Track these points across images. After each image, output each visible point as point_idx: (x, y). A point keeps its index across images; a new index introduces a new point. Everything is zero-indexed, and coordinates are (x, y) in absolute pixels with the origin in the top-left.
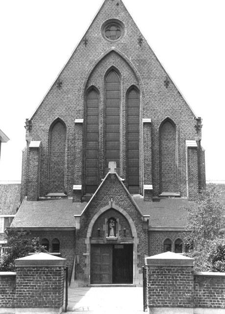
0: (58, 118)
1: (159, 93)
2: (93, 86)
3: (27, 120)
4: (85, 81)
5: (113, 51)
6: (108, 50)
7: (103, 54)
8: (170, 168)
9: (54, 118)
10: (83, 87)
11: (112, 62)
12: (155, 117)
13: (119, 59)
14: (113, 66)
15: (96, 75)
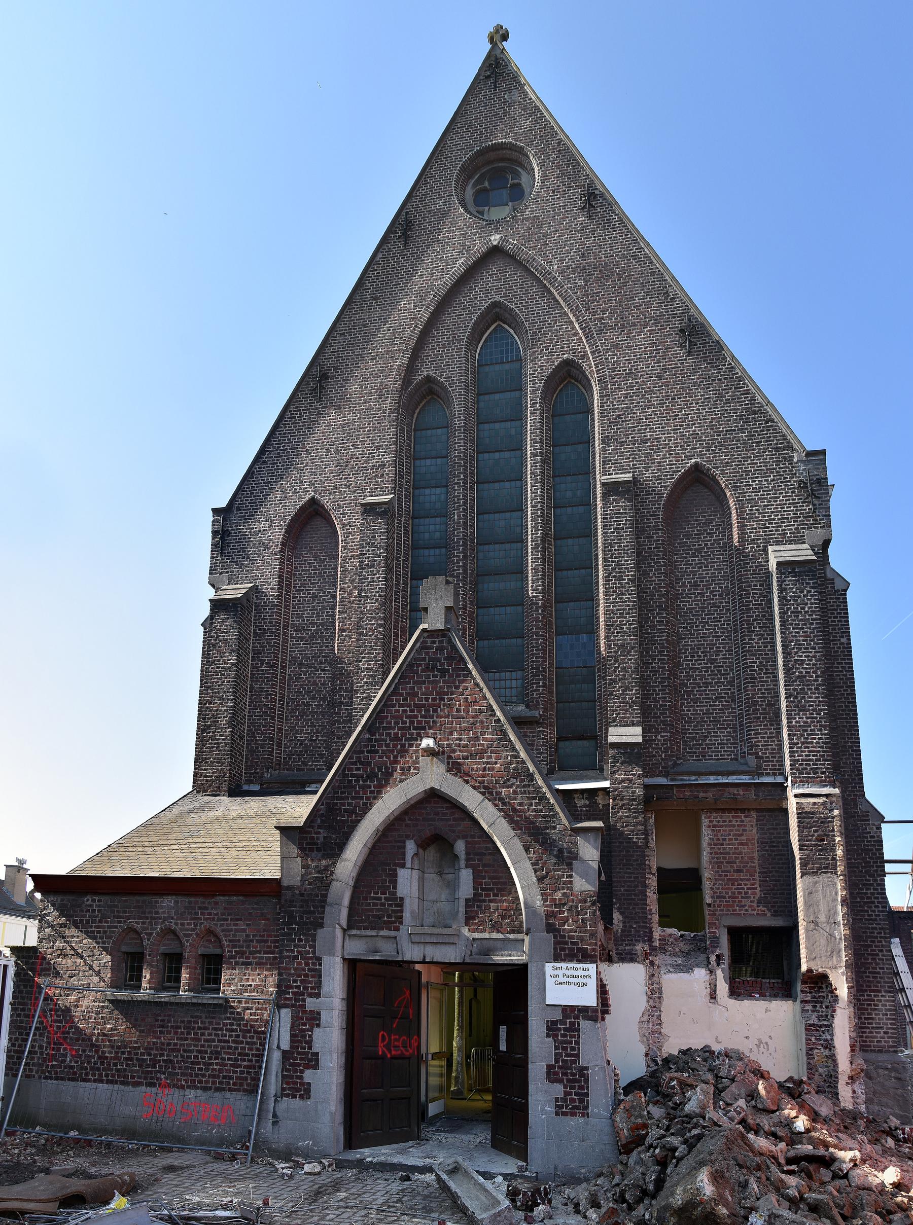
0: (313, 501)
1: (660, 377)
2: (428, 379)
3: (216, 511)
4: (401, 361)
5: (495, 252)
6: (478, 247)
7: (461, 265)
8: (712, 661)
9: (300, 498)
10: (393, 382)
11: (491, 288)
12: (647, 469)
13: (515, 277)
14: (495, 305)
15: (440, 337)
